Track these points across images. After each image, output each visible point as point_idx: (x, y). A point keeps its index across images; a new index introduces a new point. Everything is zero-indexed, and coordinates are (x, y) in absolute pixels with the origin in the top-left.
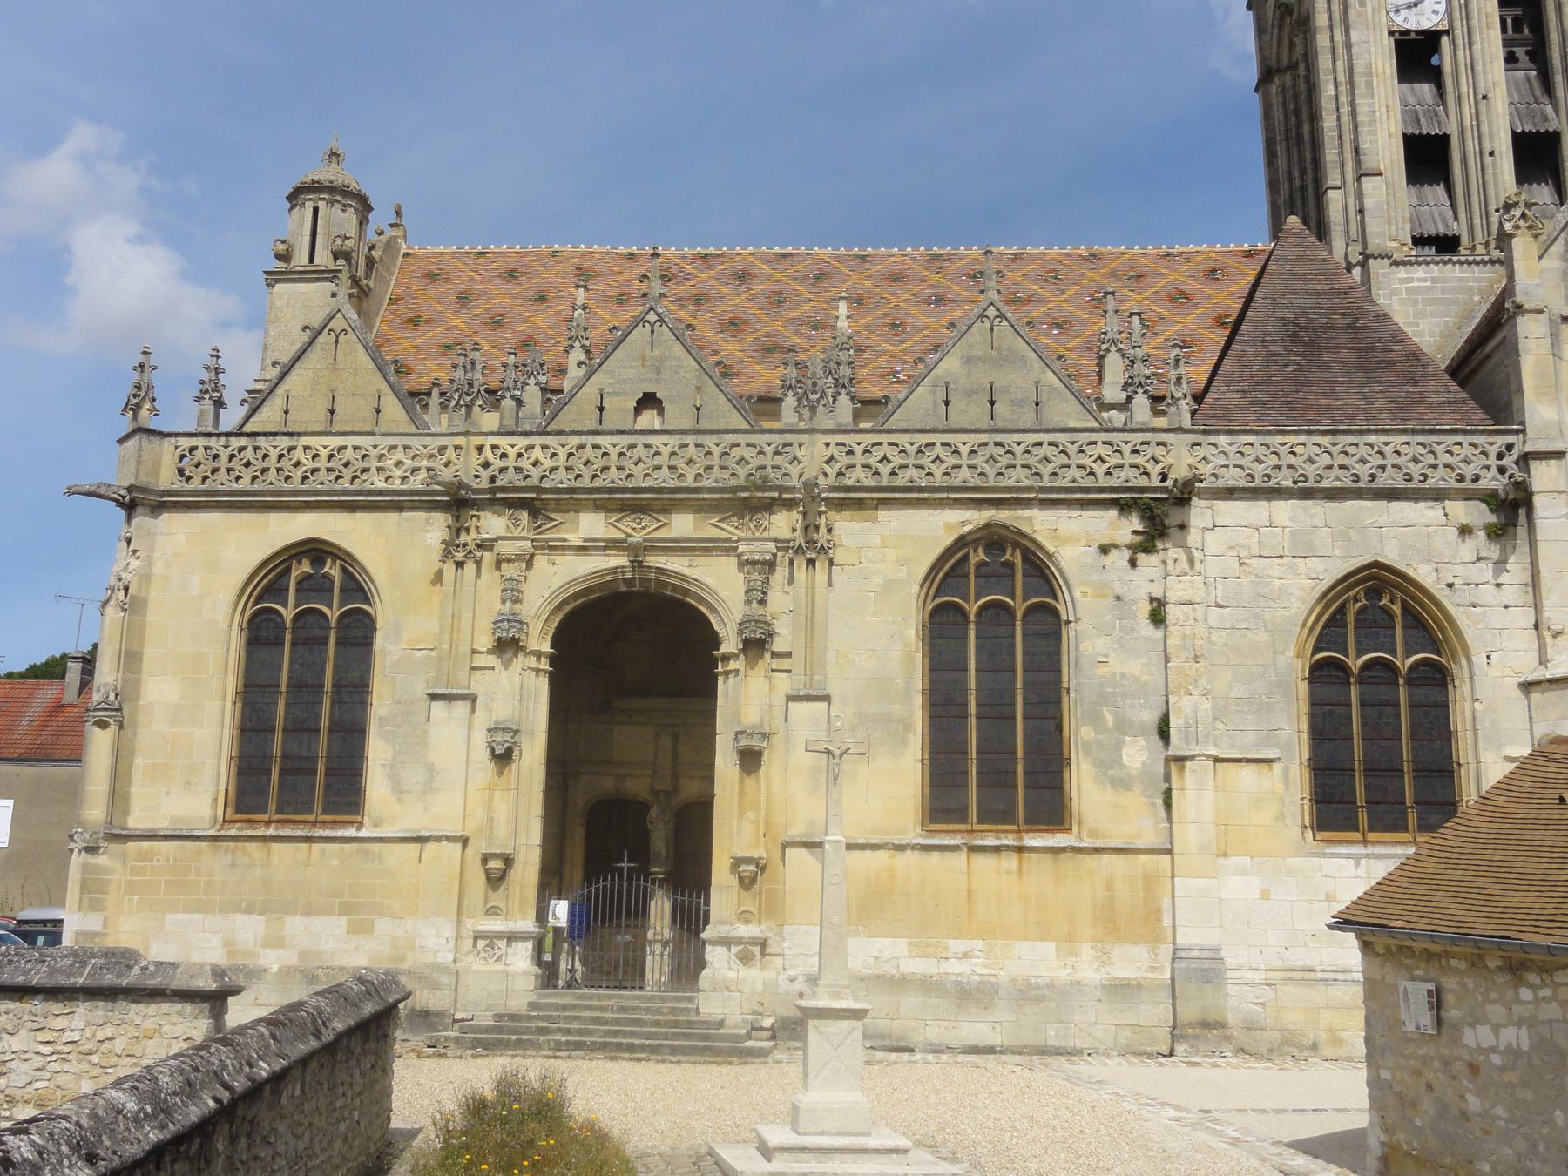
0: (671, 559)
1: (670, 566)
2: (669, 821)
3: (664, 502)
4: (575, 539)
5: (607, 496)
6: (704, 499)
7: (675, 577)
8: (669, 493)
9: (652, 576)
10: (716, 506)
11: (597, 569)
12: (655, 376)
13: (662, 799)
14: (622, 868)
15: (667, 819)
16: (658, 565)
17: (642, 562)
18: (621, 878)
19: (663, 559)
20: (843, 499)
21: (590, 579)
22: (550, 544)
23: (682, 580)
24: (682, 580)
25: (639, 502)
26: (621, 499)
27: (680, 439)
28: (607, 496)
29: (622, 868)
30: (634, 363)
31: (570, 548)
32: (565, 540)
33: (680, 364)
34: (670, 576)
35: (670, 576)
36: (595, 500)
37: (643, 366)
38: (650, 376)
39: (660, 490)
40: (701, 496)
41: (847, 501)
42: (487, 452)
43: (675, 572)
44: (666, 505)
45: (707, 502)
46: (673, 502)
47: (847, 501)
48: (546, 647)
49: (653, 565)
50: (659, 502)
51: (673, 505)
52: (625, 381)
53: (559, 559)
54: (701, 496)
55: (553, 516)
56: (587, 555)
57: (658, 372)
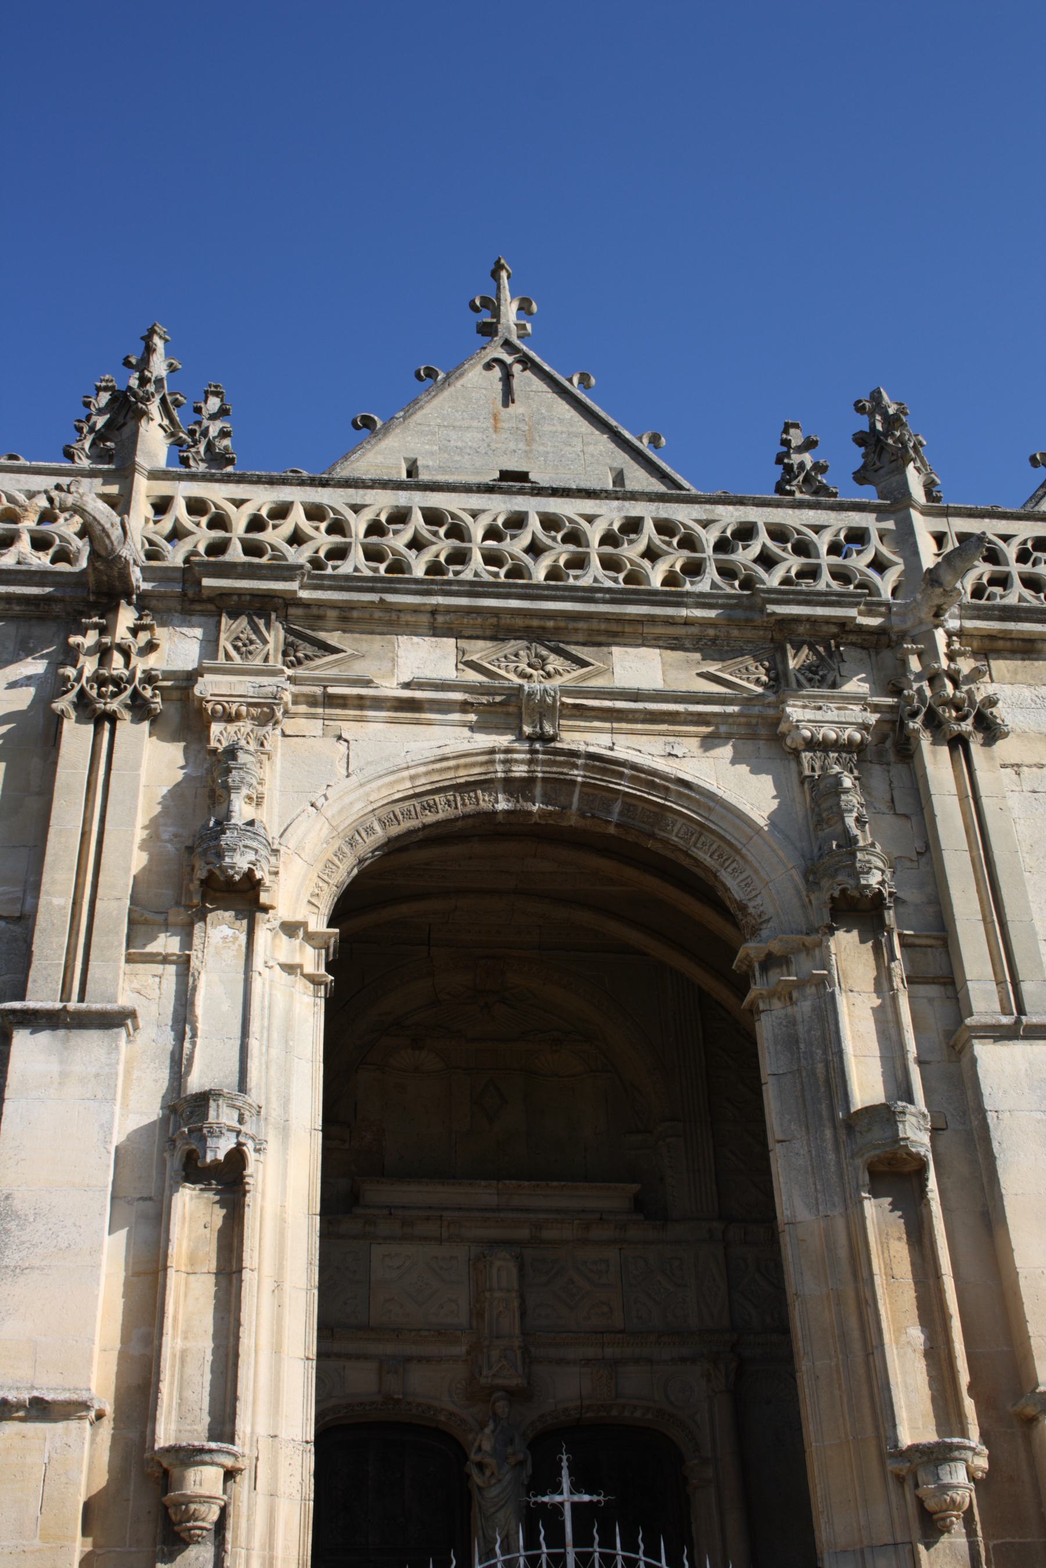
0: (621, 740)
1: (621, 753)
2: (521, 1464)
3: (595, 625)
4: (390, 688)
5: (464, 601)
6: (687, 622)
7: (633, 779)
8: (605, 602)
9: (578, 775)
10: (714, 640)
11: (446, 751)
12: (522, 446)
13: (502, 1407)
14: (558, 1508)
15: (521, 1457)
16: (592, 749)
17: (553, 739)
18: (556, 1539)
19: (605, 739)
20: (991, 637)
21: (427, 774)
22: (331, 690)
23: (652, 785)
24: (652, 785)
25: (535, 623)
26: (496, 612)
27: (620, 509)
28: (464, 601)
29: (558, 1508)
30: (475, 424)
31: (377, 703)
32: (367, 683)
33: (574, 429)
34: (621, 775)
35: (621, 775)
36: (434, 611)
37: (496, 429)
38: (512, 446)
39: (588, 594)
40: (684, 612)
41: (1001, 644)
42: (179, 509)
43: (634, 767)
44: (599, 632)
45: (694, 630)
46: (614, 627)
47: (1001, 644)
48: (318, 923)
49: (582, 748)
50: (581, 625)
51: (615, 634)
52: (460, 450)
53: (349, 730)
54: (684, 612)
55: (333, 638)
56: (418, 722)
57: (529, 442)
